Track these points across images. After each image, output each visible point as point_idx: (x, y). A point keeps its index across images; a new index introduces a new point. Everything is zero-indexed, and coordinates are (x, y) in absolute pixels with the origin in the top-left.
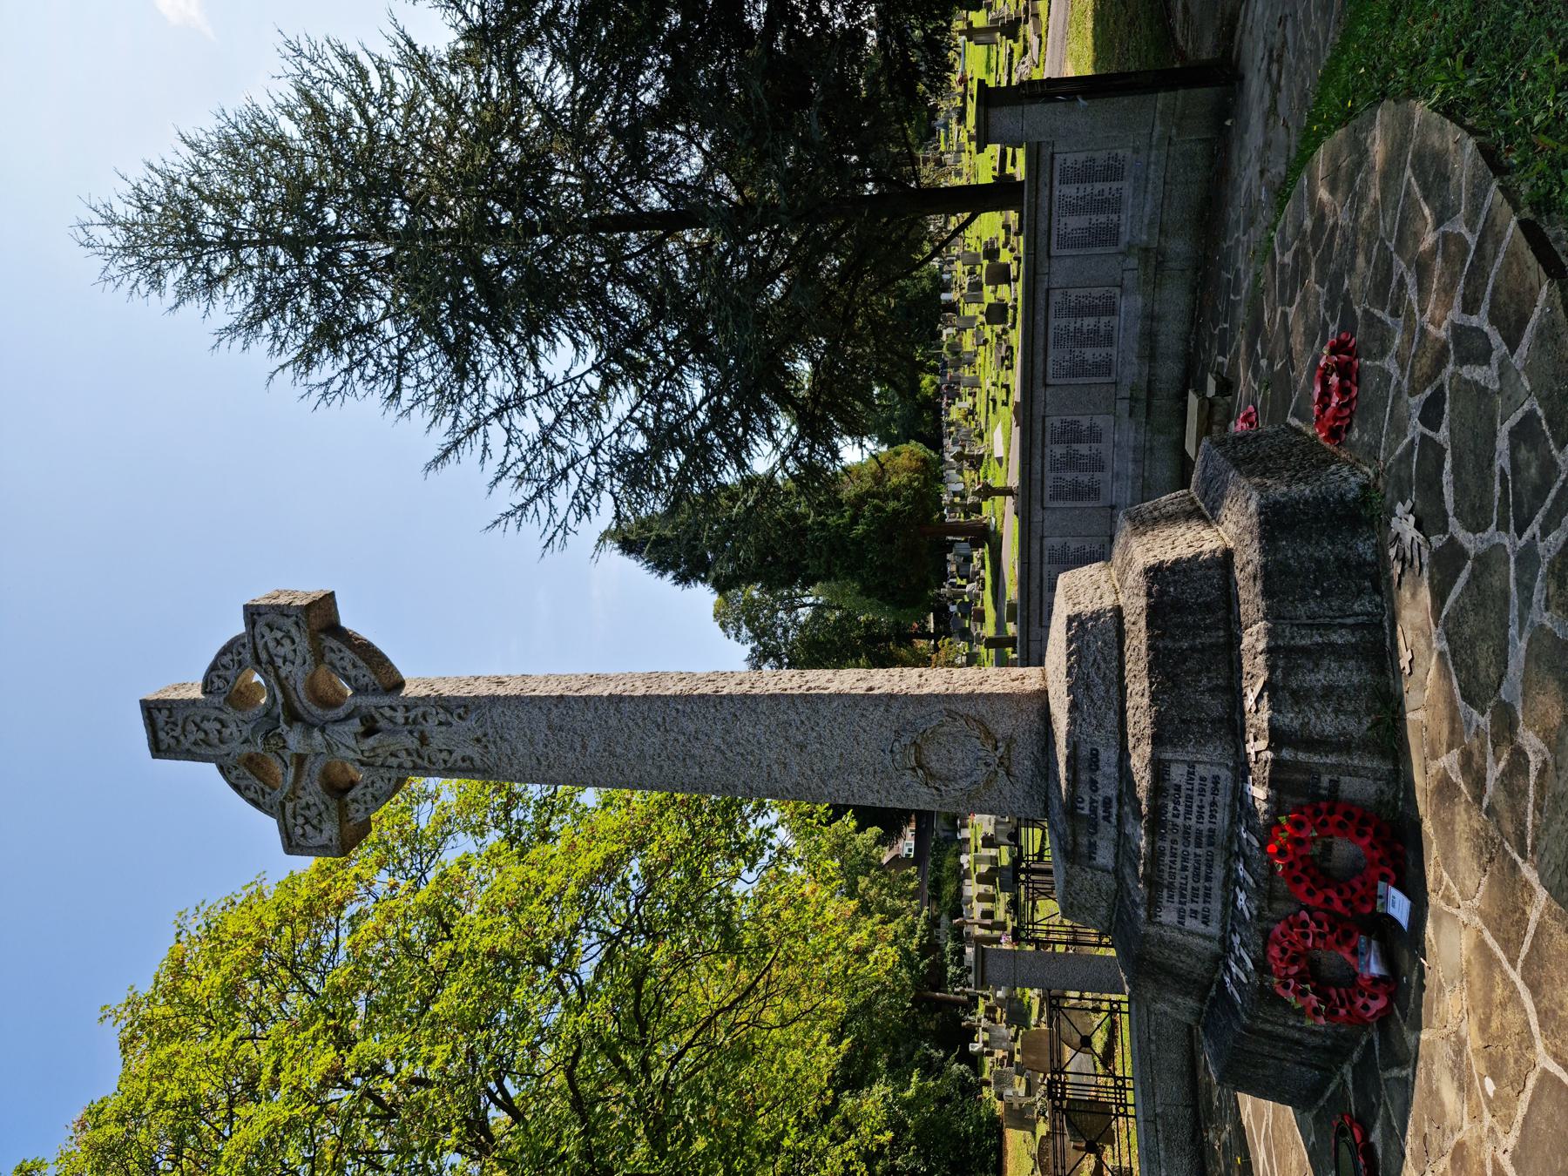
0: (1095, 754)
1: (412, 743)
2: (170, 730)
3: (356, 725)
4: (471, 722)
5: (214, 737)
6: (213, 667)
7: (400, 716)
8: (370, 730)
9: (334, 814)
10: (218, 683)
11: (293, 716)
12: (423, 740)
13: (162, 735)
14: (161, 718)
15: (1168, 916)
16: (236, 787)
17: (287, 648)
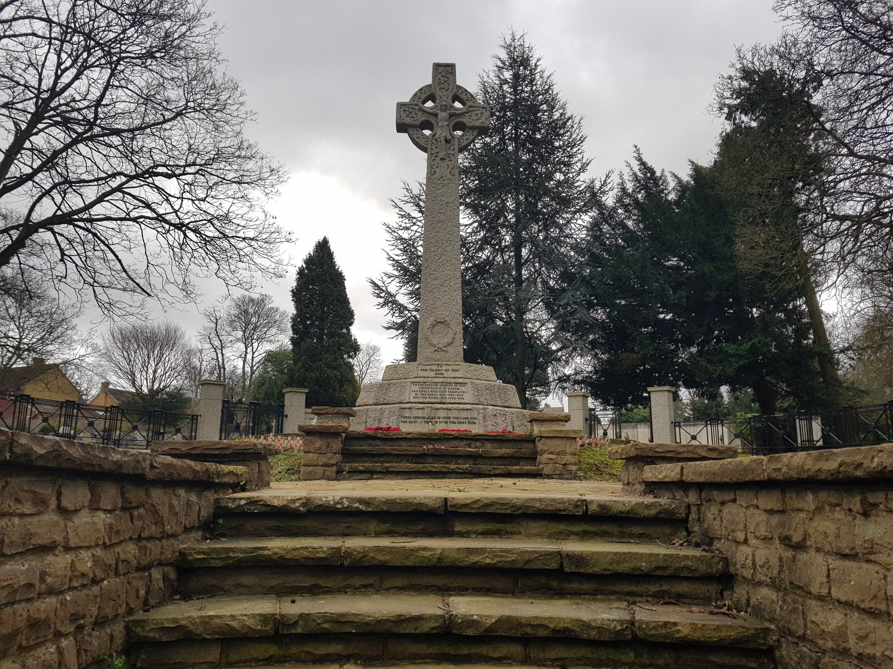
0: (458, 371)
1: (441, 155)
2: (444, 72)
3: (449, 137)
4: (449, 176)
5: (442, 86)
6: (466, 91)
7: (451, 152)
8: (447, 141)
9: (414, 123)
10: (460, 91)
11: (451, 116)
12: (442, 159)
13: (442, 68)
14: (449, 69)
15: (414, 388)
16: (421, 89)
17: (474, 117)
